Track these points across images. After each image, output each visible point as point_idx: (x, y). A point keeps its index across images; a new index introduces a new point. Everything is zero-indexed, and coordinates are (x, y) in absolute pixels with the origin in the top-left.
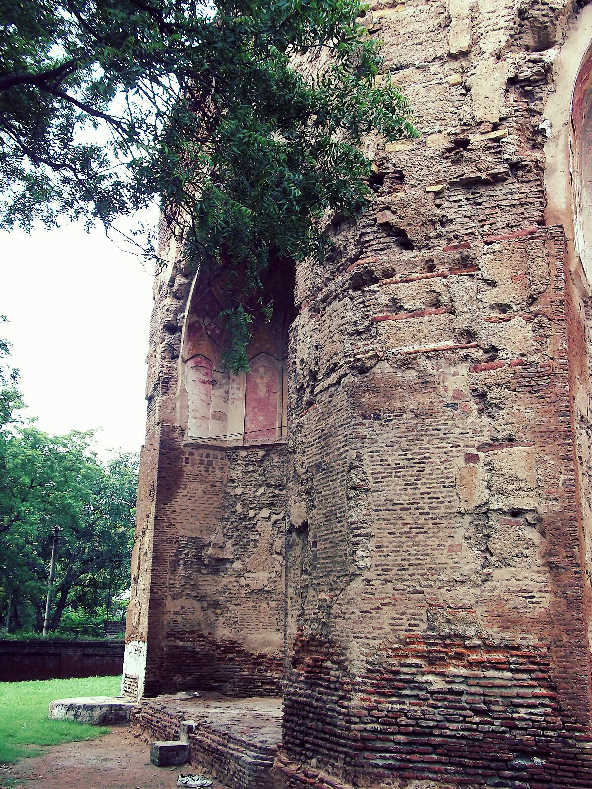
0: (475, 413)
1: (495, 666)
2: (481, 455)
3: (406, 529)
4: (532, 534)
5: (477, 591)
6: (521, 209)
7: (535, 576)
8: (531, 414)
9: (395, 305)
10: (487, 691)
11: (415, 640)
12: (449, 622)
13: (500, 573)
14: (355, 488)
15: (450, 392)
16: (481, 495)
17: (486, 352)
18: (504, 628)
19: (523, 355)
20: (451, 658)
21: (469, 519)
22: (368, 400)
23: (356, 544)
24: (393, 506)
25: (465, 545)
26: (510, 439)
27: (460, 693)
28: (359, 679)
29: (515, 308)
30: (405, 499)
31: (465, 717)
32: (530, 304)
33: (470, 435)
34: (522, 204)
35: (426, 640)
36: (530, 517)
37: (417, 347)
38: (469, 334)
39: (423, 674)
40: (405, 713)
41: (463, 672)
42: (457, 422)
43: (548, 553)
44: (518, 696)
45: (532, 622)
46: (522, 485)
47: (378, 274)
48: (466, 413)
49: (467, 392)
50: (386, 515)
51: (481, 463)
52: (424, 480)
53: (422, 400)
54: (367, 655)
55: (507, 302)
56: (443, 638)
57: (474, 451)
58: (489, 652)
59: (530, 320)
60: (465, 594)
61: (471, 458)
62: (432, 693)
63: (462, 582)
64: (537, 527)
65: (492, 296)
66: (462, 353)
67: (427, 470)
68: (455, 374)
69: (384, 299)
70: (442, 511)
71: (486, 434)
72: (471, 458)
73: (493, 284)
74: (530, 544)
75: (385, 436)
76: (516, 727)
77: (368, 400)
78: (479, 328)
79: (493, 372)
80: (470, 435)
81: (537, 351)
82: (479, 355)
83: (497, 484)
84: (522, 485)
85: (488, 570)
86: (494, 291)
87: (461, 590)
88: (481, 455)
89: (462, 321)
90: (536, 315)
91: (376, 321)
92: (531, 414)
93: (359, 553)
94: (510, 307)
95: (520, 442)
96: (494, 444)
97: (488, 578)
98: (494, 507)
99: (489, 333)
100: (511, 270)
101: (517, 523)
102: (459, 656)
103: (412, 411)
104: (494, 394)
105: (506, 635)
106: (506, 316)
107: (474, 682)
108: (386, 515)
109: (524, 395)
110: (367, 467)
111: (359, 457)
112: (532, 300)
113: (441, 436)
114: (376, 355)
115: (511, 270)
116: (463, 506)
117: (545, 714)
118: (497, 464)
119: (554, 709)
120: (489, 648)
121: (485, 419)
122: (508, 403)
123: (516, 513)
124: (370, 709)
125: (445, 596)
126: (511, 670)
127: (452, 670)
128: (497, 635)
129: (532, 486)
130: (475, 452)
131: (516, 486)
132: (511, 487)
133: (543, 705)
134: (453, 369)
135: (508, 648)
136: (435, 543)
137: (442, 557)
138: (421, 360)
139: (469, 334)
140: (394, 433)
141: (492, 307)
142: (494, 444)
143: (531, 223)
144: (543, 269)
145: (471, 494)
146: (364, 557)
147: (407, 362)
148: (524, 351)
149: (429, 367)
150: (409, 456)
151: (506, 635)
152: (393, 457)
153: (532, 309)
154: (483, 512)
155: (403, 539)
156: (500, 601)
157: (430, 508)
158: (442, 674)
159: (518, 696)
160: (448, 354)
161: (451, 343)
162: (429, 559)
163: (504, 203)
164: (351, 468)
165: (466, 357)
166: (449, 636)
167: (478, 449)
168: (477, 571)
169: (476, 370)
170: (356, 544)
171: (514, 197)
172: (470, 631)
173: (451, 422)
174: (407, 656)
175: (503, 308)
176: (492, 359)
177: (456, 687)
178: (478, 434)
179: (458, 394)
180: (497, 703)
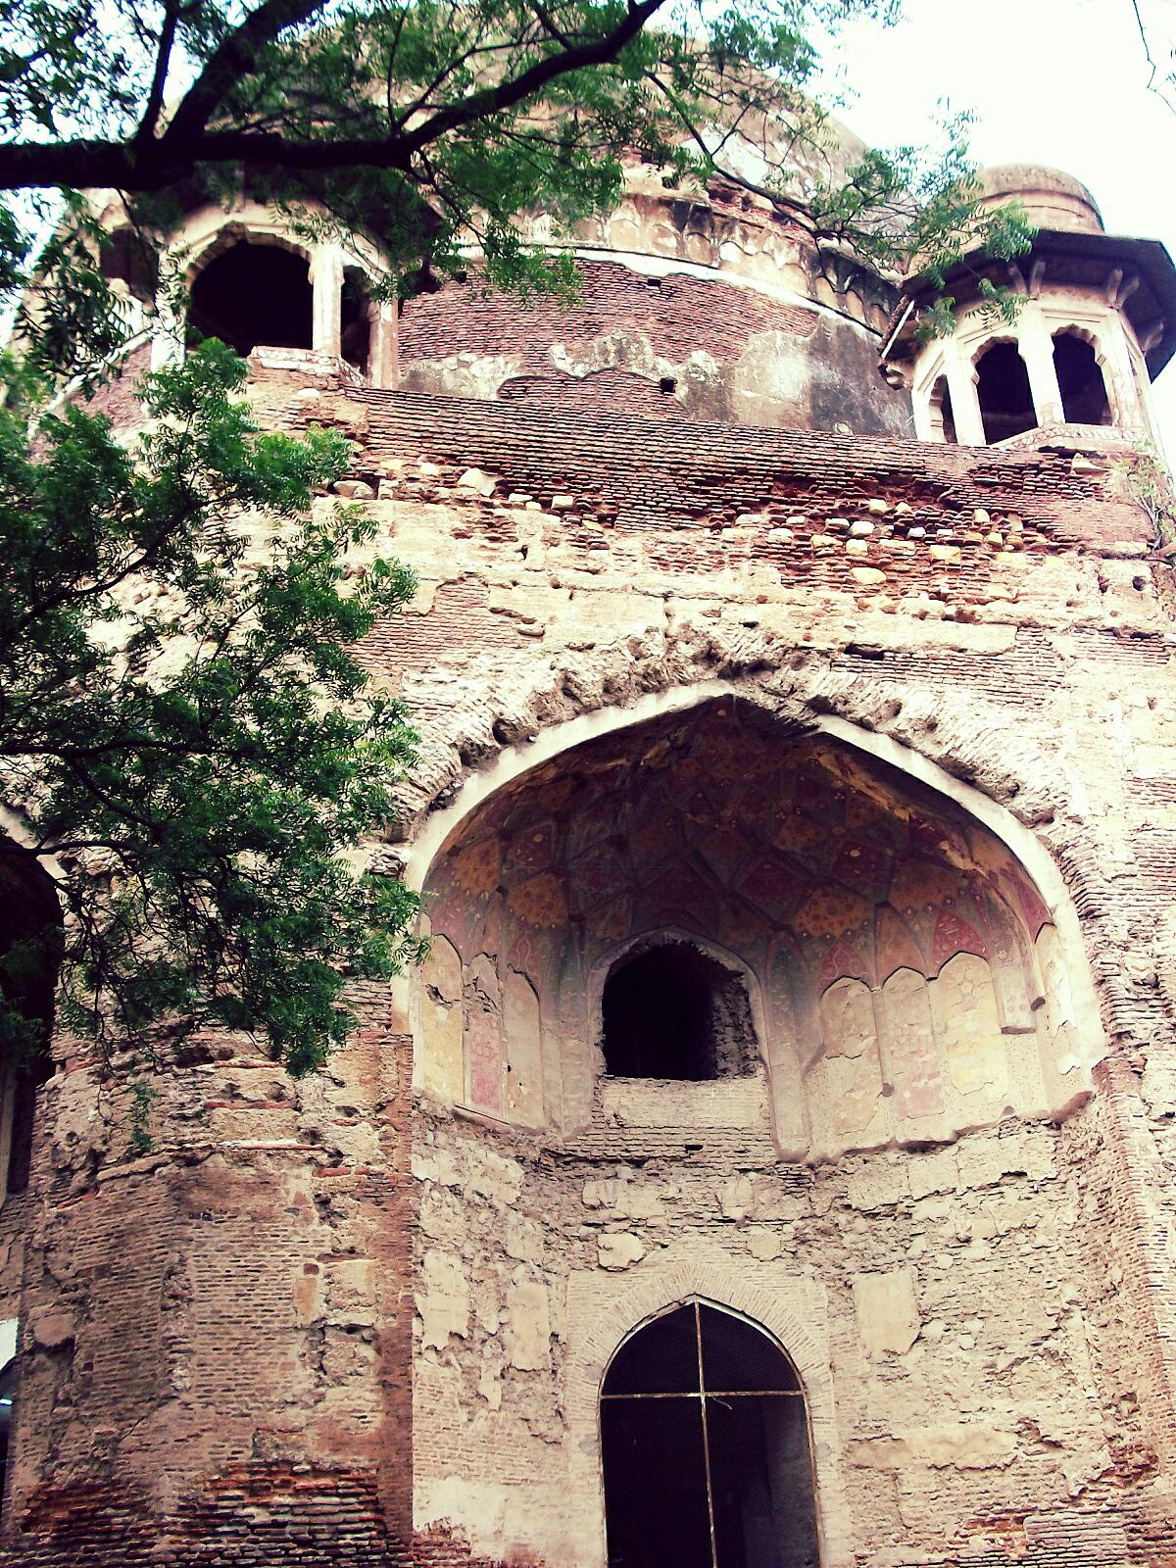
0: (317, 1220)
1: (322, 1491)
2: (321, 1265)
3: (234, 1344)
4: (367, 1352)
5: (309, 1412)
6: (370, 1009)
7: (368, 1395)
8: (374, 1226)
9: (232, 1092)
10: (314, 1519)
11: (238, 1468)
12: (277, 1447)
13: (334, 1393)
14: (174, 1297)
15: (292, 1197)
16: (320, 1309)
17: (330, 1156)
18: (336, 1451)
19: (368, 1163)
20: (276, 1487)
21: (304, 1334)
22: (198, 1196)
23: (173, 1361)
24: (220, 1319)
25: (298, 1363)
26: (352, 1251)
27: (284, 1524)
28: (169, 1519)
29: (362, 1112)
30: (235, 1312)
31: (287, 1549)
32: (378, 1111)
33: (311, 1243)
34: (371, 1003)
35: (250, 1469)
36: (366, 1334)
37: (254, 1143)
38: (314, 1136)
39: (244, 1506)
40: (219, 1552)
41: (289, 1500)
42: (298, 1229)
43: (384, 1371)
44: (345, 1522)
45: (363, 1443)
46: (362, 1300)
47: (214, 1053)
48: (308, 1220)
49: (310, 1198)
50: (212, 1328)
51: (320, 1275)
52: (257, 1291)
53: (259, 1201)
54: (180, 1489)
55: (354, 1106)
56: (269, 1465)
57: (313, 1261)
58: (316, 1477)
59: (376, 1128)
60: (296, 1416)
61: (311, 1269)
62: (253, 1527)
63: (293, 1403)
64: (373, 1343)
65: (340, 1097)
66: (307, 1155)
67: (262, 1280)
68: (298, 1177)
69: (222, 1084)
70: (276, 1325)
71: (328, 1244)
72: (311, 1269)
73: (341, 1084)
74: (365, 1362)
75: (216, 1239)
76: (342, 1555)
77: (198, 1196)
78: (324, 1129)
79: (338, 1178)
80: (311, 1243)
81: (383, 1161)
82: (323, 1158)
83: (336, 1298)
84: (362, 1300)
85: (322, 1389)
86: (341, 1091)
87: (291, 1411)
88: (321, 1265)
89: (308, 1121)
90: (384, 1124)
91: (210, 1107)
92: (374, 1226)
93: (178, 1372)
94: (356, 1111)
95: (362, 1255)
96: (335, 1255)
97: (321, 1398)
98: (332, 1322)
99: (336, 1135)
100: (359, 1072)
101: (353, 1340)
102: (285, 1484)
103: (248, 1213)
104: (338, 1202)
105: (337, 1458)
106: (352, 1119)
107: (299, 1510)
108: (212, 1328)
109: (367, 1206)
110: (192, 1273)
111: (182, 1262)
112: (380, 1108)
113: (279, 1243)
114: (210, 1146)
115: (359, 1072)
116: (300, 1320)
117: (371, 1538)
118: (337, 1277)
119: (379, 1532)
120: (317, 1472)
121: (327, 1227)
122: (352, 1213)
123: (352, 1329)
124: (178, 1553)
125: (275, 1418)
126: (338, 1495)
127: (277, 1499)
128: (327, 1458)
129: (371, 1301)
130: (316, 1263)
131: (355, 1300)
132: (350, 1301)
133: (368, 1529)
134: (296, 1171)
135: (338, 1472)
136: (267, 1360)
137: (273, 1376)
138: (262, 1157)
139: (314, 1136)
140: (225, 1236)
141: (338, 1109)
142: (335, 1255)
143: (380, 1025)
144: (394, 1077)
145: (308, 1307)
146: (183, 1377)
147: (245, 1159)
148: (370, 1159)
149: (269, 1166)
150: (242, 1263)
151: (337, 1458)
152: (223, 1263)
153: (379, 1116)
154: (319, 1329)
155: (231, 1356)
156: (332, 1422)
157: (264, 1322)
158: (267, 1506)
159: (345, 1522)
160: (291, 1154)
161: (294, 1142)
162: (258, 1378)
163: (354, 999)
164: (170, 1273)
165: (310, 1160)
166: (276, 1463)
167: (319, 1259)
168: (310, 1391)
169: (320, 1174)
170: (173, 1361)
171: (364, 994)
172: (300, 1456)
173: (290, 1229)
174: (226, 1489)
175: (350, 1111)
176: (335, 1165)
177: (280, 1518)
178: (319, 1243)
179: (300, 1199)
180: (322, 1531)
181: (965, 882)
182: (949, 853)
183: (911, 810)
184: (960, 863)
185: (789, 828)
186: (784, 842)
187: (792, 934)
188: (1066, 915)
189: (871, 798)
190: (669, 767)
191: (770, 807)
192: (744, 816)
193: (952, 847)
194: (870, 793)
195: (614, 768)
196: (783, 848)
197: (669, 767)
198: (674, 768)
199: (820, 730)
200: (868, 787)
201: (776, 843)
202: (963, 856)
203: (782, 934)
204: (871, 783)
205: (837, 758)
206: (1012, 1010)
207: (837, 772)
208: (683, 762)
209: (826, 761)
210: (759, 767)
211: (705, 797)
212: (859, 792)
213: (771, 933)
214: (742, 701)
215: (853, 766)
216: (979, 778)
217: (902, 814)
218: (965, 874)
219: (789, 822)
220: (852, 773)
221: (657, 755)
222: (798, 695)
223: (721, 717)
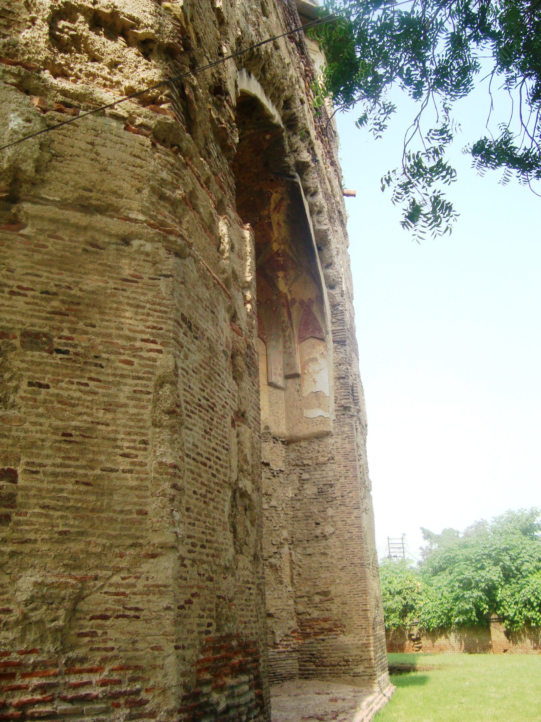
181: (275, 298)
182: (280, 279)
183: (282, 247)
184: (282, 286)
188: (330, 337)
189: (272, 229)
193: (285, 277)
194: (275, 227)
199: (295, 180)
200: (278, 223)
202: (286, 284)
204: (281, 223)
205: (282, 199)
206: (275, 374)
207: (273, 206)
209: (275, 197)
210: (244, 178)
212: (270, 224)
214: (282, 138)
215: (283, 208)
216: (325, 251)
217: (275, 247)
218: (279, 294)
220: (278, 212)
222: (296, 155)
223: (264, 139)
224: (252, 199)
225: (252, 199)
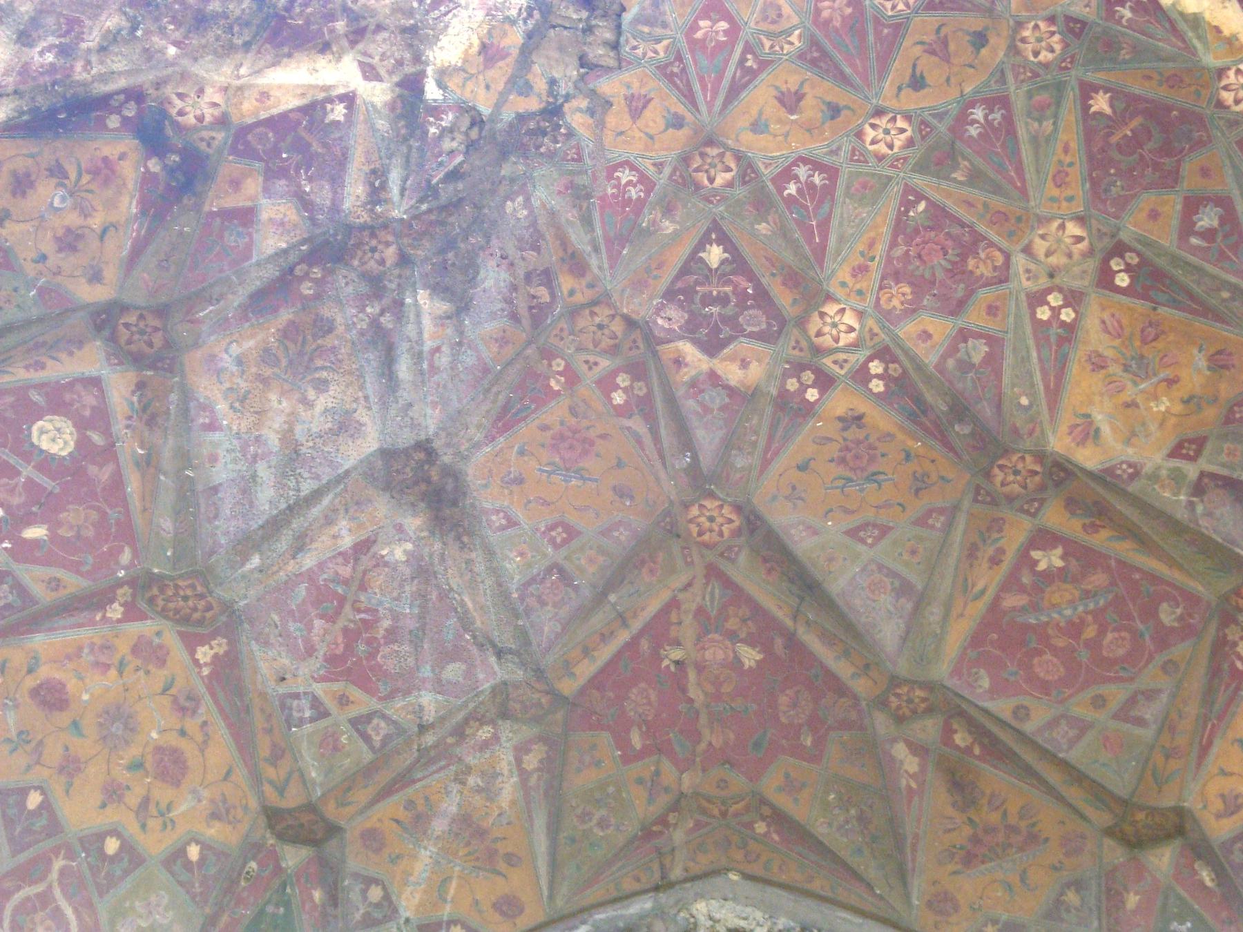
185: (1098, 363)
186: (1087, 433)
187: (1201, 850)
190: (553, 112)
191: (1003, 276)
192: (907, 330)
195: (313, 110)
196: (1088, 458)
197: (553, 112)
198: (576, 118)
201: (1058, 442)
203: (1163, 860)
208: (608, 86)
210: (917, 83)
211: (737, 263)
213: (1115, 854)
219: (1094, 337)
221: (488, 52)
224: (1101, 103)
225: (1101, 103)
